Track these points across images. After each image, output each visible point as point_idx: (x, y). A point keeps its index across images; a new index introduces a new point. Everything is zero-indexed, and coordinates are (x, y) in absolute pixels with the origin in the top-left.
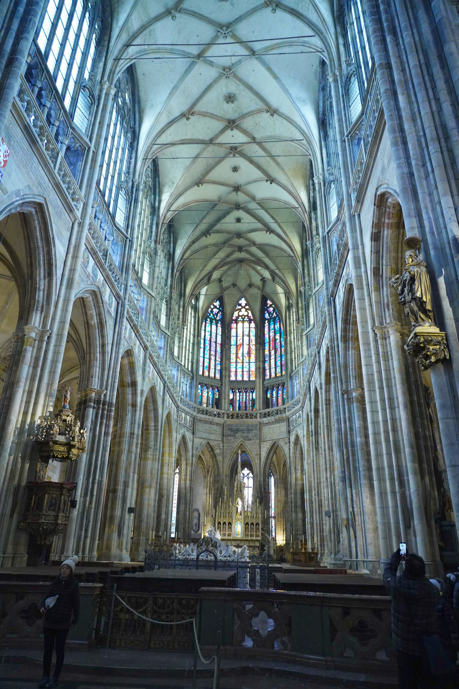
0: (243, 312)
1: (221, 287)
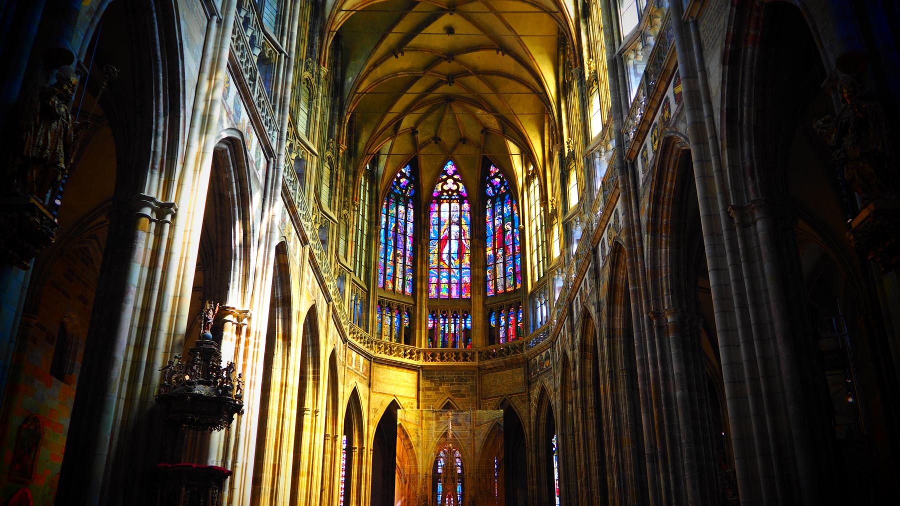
0: (450, 185)
1: (414, 142)
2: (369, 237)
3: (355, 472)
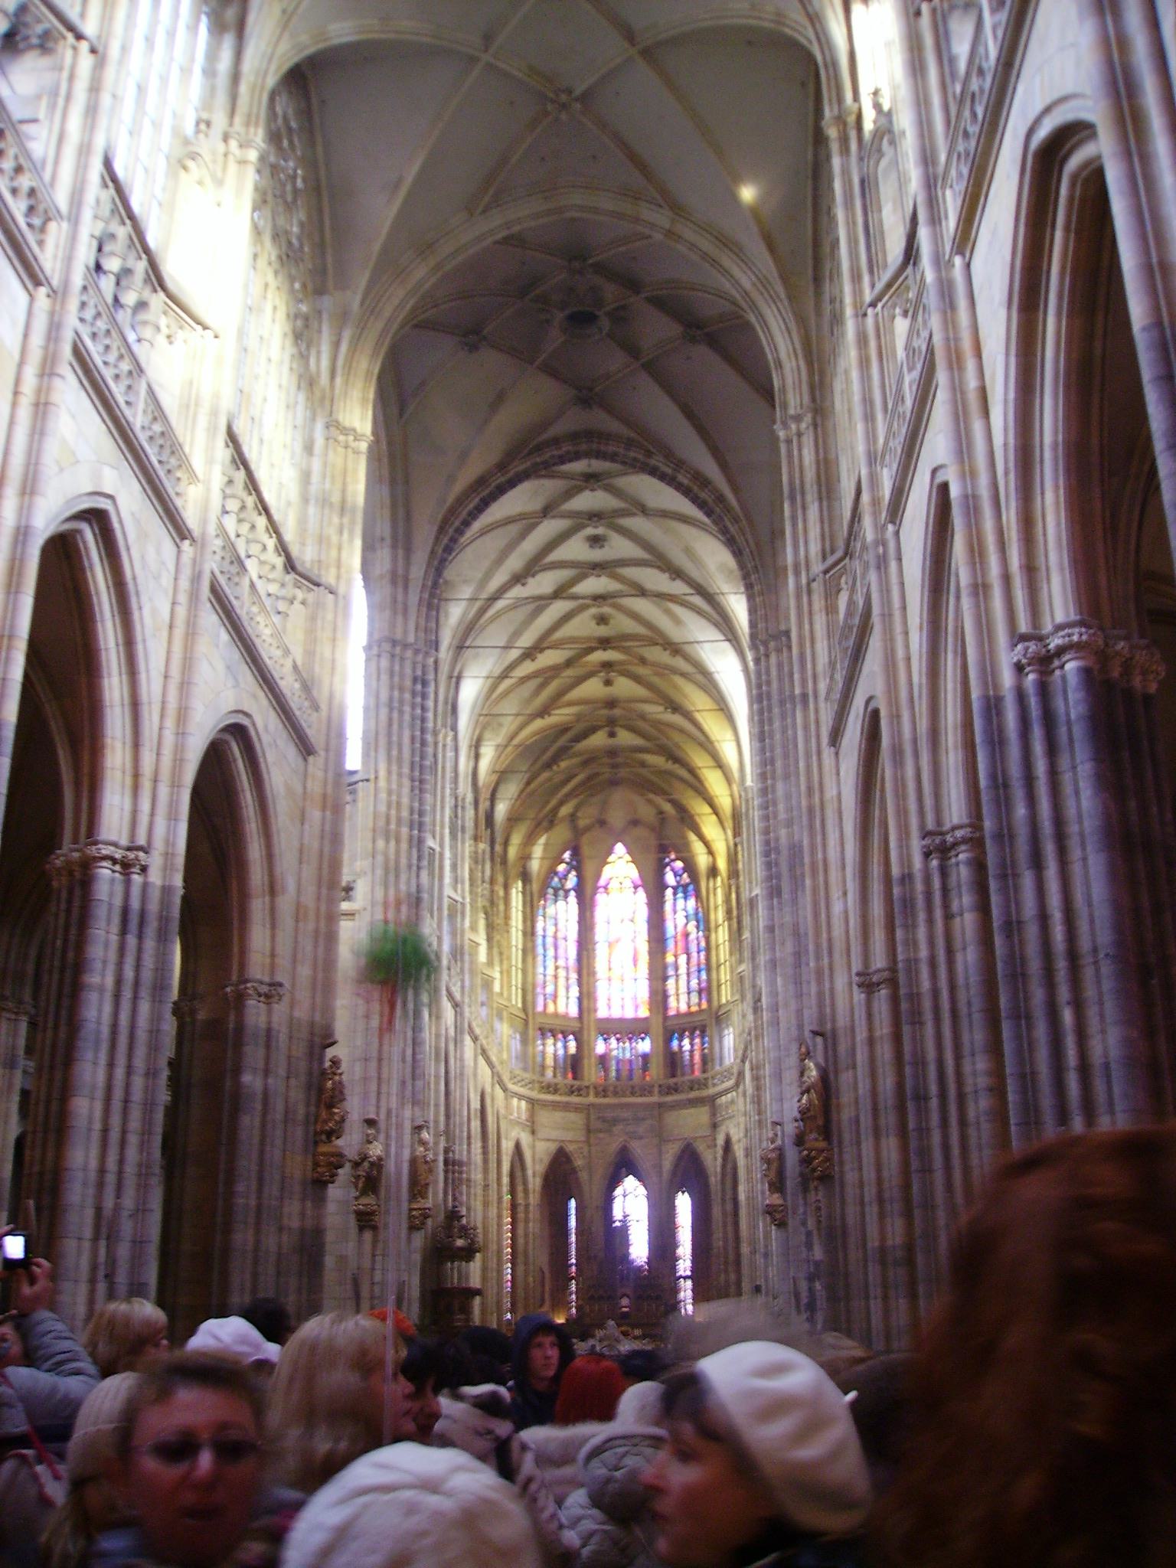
2: (524, 951)
3: (520, 1231)
